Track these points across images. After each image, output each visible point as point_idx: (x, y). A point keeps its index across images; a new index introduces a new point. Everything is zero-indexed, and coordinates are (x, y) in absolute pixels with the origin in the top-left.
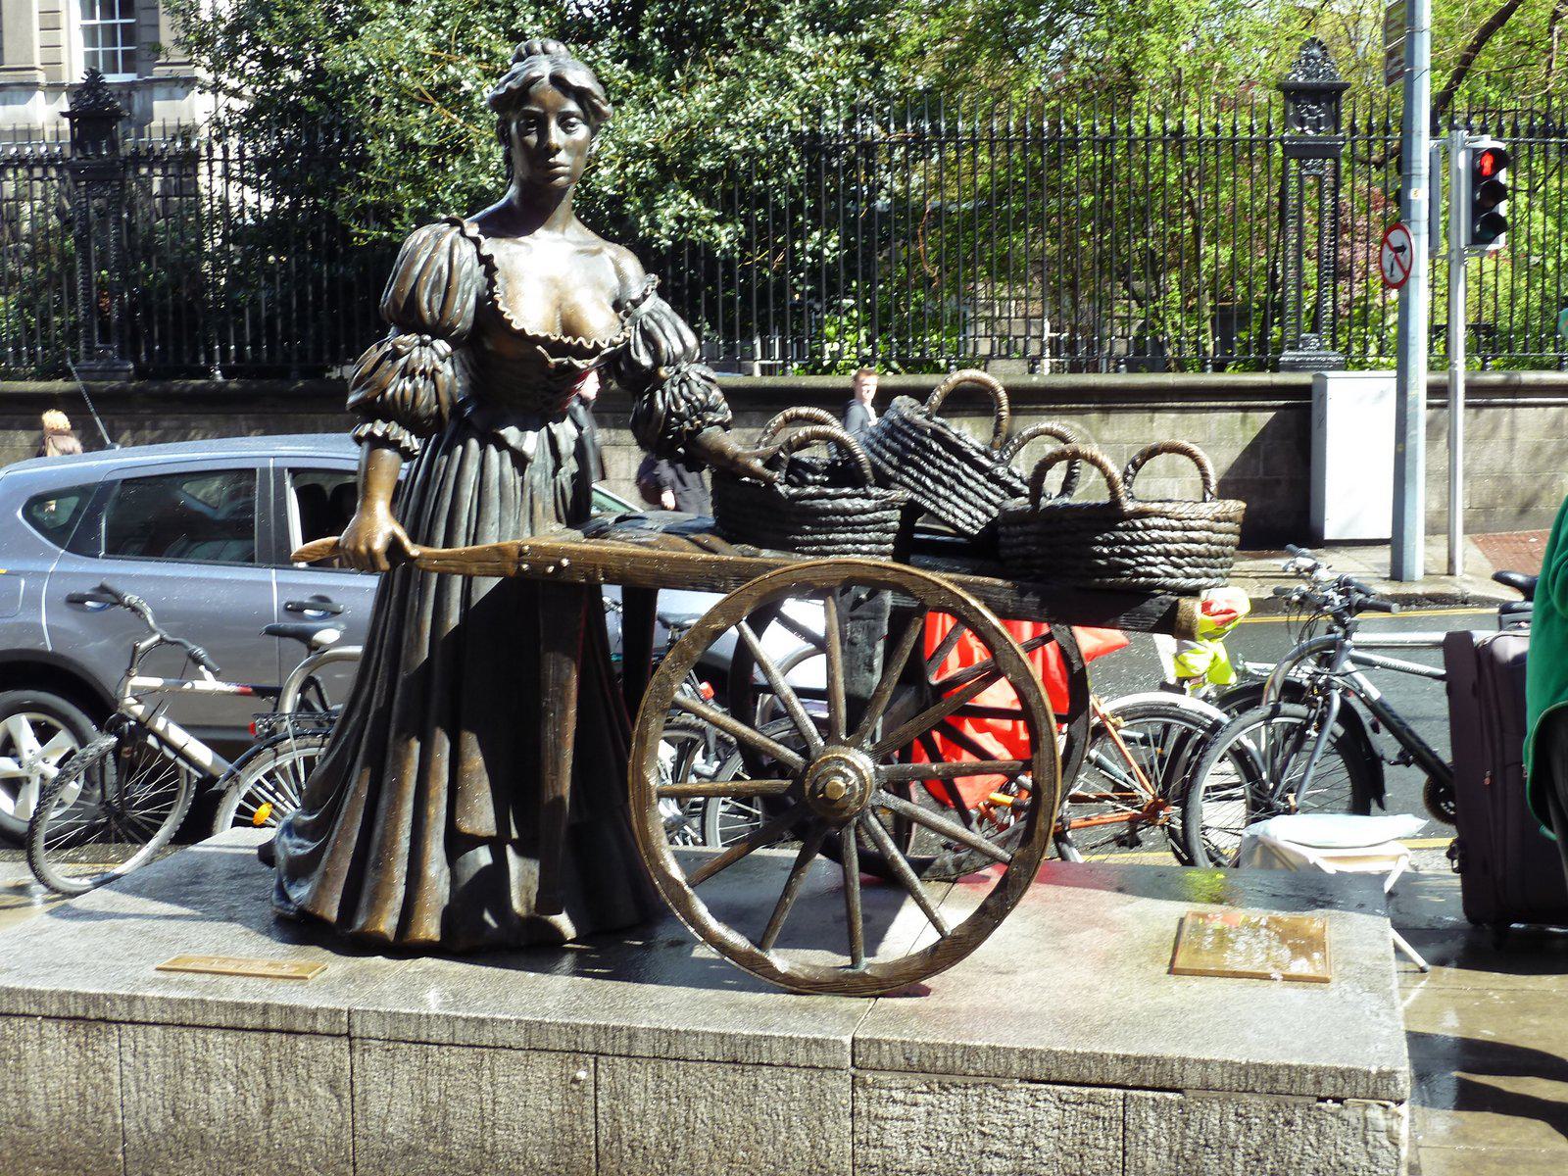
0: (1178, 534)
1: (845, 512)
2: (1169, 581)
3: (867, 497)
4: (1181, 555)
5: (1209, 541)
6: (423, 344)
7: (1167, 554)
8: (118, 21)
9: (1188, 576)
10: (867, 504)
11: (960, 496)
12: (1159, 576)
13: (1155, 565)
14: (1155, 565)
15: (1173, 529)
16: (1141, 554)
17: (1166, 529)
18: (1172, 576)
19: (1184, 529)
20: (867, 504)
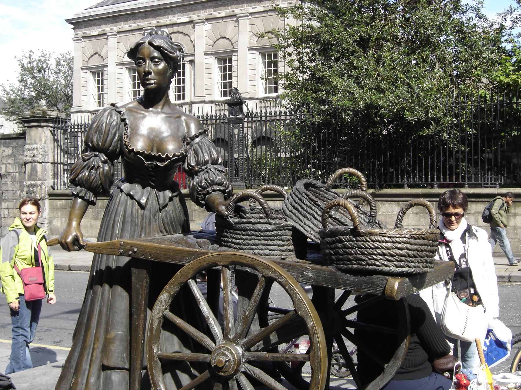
0: (390, 245)
1: (260, 230)
2: (385, 269)
3: (270, 224)
4: (391, 255)
5: (408, 249)
6: (96, 156)
7: (384, 254)
8: (228, 81)
9: (397, 266)
10: (269, 227)
11: (315, 225)
12: (379, 266)
13: (377, 260)
14: (377, 260)
15: (387, 242)
16: (369, 254)
17: (383, 242)
18: (387, 266)
19: (393, 242)
20: (269, 227)
